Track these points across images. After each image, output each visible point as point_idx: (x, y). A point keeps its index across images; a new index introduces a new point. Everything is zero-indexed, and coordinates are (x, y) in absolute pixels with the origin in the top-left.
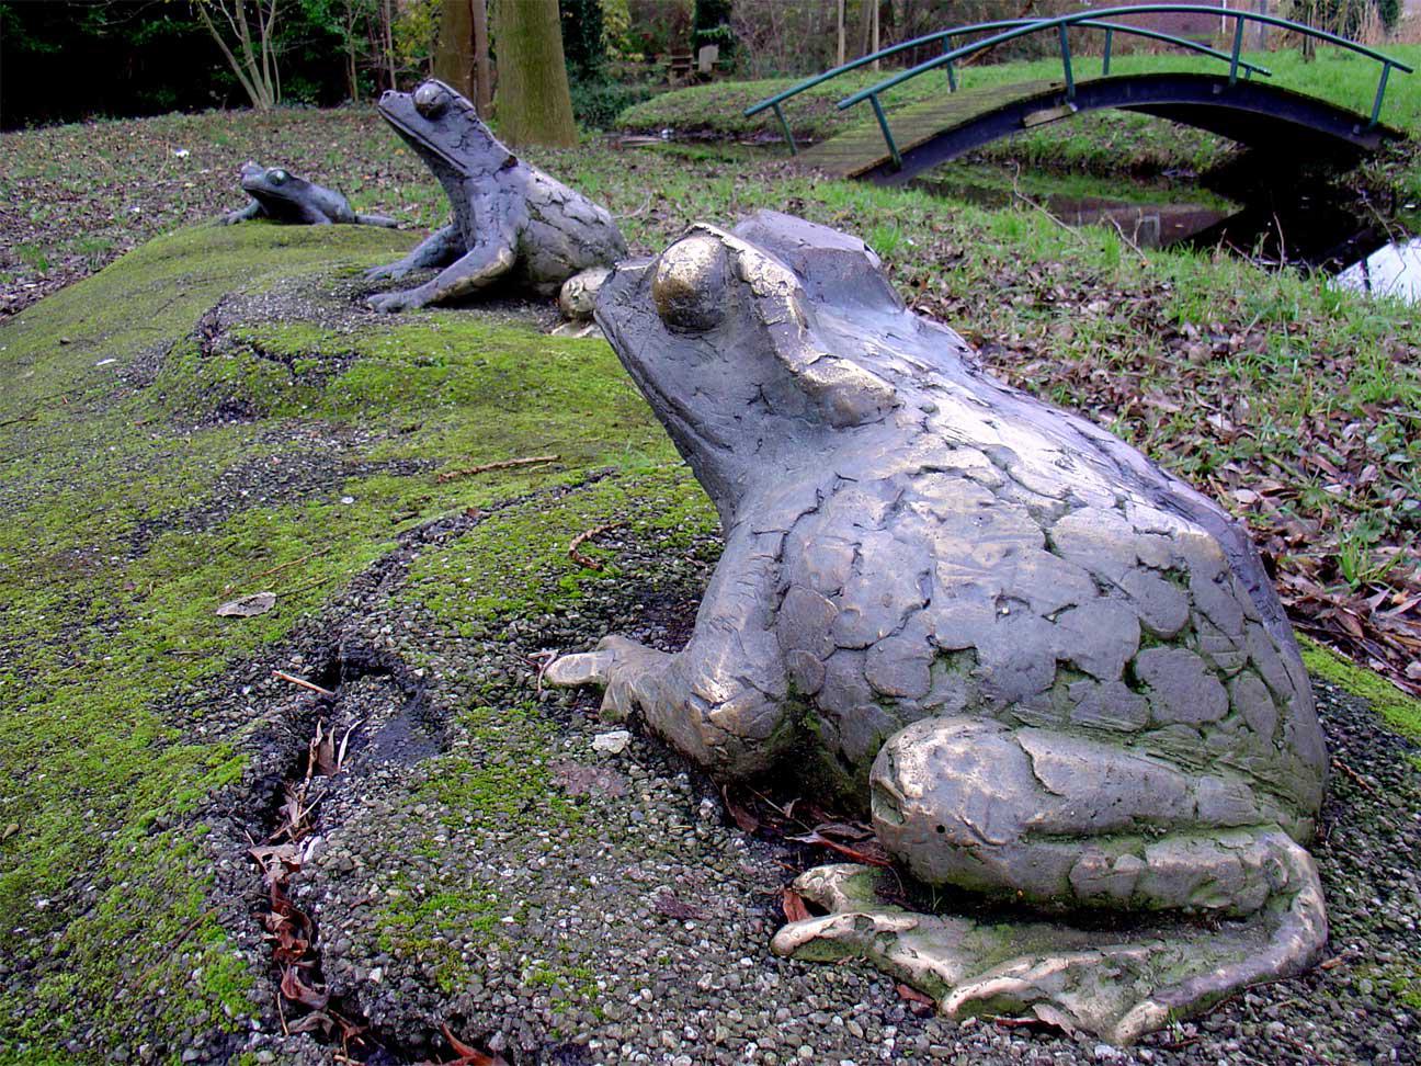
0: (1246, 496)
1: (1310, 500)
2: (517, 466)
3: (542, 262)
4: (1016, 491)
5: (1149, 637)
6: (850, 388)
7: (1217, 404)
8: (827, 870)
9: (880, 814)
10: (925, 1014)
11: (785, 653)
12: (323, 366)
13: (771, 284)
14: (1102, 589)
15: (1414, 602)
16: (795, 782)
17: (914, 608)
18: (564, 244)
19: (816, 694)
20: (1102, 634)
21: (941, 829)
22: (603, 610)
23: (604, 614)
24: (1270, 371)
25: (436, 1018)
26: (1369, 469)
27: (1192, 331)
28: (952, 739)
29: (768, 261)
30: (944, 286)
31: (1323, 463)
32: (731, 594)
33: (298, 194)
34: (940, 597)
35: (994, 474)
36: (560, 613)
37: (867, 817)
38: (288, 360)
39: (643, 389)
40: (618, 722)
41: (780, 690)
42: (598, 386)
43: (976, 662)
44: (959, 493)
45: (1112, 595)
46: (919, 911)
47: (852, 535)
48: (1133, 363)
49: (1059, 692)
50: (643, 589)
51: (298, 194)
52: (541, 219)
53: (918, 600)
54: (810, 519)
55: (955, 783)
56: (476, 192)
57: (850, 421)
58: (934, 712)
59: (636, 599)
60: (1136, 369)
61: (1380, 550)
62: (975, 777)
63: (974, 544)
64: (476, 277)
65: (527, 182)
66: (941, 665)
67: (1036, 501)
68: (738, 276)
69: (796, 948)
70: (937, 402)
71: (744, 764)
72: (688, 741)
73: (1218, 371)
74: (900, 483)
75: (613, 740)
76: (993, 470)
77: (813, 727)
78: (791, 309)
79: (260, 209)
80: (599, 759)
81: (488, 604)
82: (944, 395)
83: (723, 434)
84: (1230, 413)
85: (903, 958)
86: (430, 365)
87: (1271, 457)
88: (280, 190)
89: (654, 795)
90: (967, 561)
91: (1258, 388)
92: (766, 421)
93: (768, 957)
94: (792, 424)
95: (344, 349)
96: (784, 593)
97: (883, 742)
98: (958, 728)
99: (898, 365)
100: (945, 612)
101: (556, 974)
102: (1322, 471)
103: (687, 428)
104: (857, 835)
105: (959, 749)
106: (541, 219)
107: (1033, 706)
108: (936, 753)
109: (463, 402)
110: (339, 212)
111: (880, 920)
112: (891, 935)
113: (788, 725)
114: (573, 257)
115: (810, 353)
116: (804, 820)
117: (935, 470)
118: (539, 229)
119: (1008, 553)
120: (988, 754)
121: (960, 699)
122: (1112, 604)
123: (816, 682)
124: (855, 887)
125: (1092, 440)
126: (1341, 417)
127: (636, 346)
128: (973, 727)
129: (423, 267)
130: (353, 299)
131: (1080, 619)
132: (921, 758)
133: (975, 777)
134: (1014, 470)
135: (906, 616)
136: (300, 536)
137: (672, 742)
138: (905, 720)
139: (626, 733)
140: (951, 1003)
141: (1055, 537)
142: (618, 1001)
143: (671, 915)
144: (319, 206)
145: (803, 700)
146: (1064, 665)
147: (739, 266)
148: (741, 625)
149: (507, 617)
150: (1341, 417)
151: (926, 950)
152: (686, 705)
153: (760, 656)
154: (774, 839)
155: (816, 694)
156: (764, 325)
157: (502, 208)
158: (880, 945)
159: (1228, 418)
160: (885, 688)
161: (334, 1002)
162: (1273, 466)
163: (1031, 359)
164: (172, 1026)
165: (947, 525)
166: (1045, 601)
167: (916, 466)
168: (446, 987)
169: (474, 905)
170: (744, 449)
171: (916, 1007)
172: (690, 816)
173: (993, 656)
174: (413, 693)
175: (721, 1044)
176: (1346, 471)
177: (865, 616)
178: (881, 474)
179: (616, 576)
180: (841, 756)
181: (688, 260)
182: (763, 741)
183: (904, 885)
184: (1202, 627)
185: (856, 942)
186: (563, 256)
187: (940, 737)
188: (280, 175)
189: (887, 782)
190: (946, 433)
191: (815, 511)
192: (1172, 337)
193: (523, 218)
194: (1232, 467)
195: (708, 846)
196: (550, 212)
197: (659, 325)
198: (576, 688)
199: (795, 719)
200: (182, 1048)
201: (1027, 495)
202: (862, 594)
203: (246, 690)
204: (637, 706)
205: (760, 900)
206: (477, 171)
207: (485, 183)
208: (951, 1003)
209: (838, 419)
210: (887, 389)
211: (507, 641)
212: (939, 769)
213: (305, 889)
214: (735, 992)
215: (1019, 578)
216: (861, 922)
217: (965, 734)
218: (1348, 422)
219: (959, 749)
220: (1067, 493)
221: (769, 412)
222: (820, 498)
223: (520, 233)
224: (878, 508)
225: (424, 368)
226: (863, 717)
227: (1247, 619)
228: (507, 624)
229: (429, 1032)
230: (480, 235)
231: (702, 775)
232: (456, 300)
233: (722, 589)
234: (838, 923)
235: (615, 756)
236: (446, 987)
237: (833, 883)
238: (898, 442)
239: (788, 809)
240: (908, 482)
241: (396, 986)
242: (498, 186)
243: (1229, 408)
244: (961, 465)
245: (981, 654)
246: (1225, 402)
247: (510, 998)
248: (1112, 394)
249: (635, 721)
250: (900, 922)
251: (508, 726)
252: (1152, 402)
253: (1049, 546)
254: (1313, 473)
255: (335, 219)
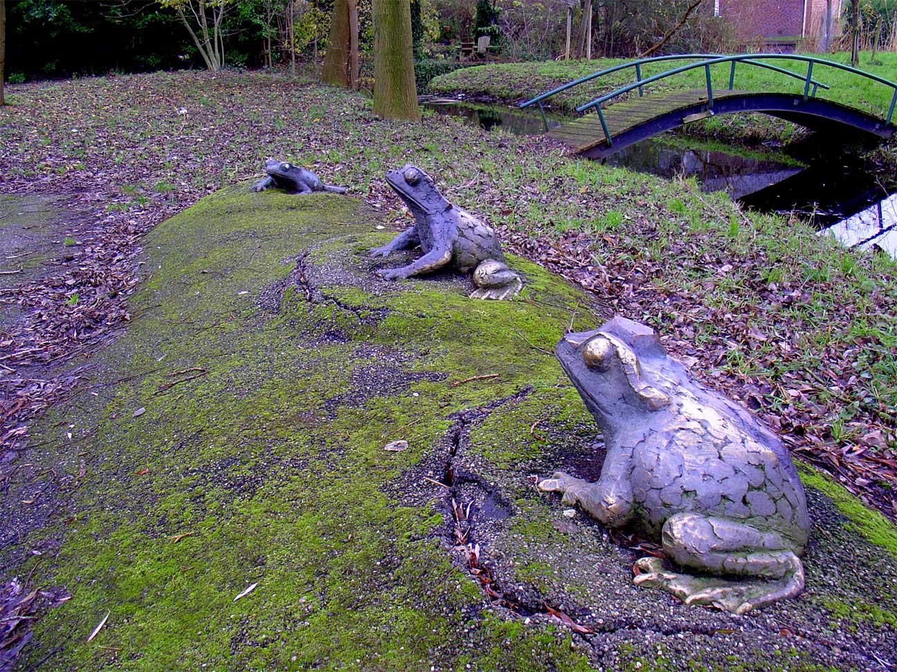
0: (794, 393)
1: (823, 396)
2: (481, 379)
3: (463, 257)
4: (709, 437)
5: (751, 488)
6: (655, 399)
7: (784, 335)
8: (647, 559)
9: (665, 542)
10: (680, 604)
11: (633, 488)
12: (374, 315)
13: (629, 360)
14: (736, 472)
15: (862, 450)
16: (637, 530)
17: (677, 477)
18: (475, 249)
19: (643, 502)
20: (736, 487)
21: (685, 548)
22: (549, 459)
23: (550, 460)
24: (811, 315)
25: (541, 601)
26: (853, 378)
27: (774, 287)
28: (689, 520)
29: (627, 350)
30: (648, 254)
31: (831, 373)
32: (614, 466)
33: (295, 175)
34: (685, 474)
35: (702, 431)
36: (534, 460)
37: (660, 542)
38: (354, 309)
39: (577, 388)
40: (571, 506)
41: (631, 500)
42: (503, 331)
43: (696, 495)
44: (691, 438)
45: (740, 474)
46: (677, 572)
47: (656, 451)
48: (744, 309)
49: (722, 506)
50: (562, 451)
51: (295, 175)
52: (464, 236)
53: (678, 475)
54: (642, 444)
55: (690, 534)
56: (433, 222)
57: (654, 409)
58: (682, 511)
59: (561, 455)
60: (745, 312)
61: (851, 424)
62: (696, 533)
63: (696, 457)
64: (433, 265)
65: (457, 218)
66: (685, 496)
67: (716, 441)
68: (617, 354)
69: (640, 583)
70: (683, 402)
71: (618, 523)
72: (599, 516)
73: (786, 314)
74: (672, 434)
75: (569, 513)
76: (702, 429)
77: (641, 512)
78: (635, 369)
79: (272, 181)
80: (566, 519)
81: (508, 455)
82: (683, 397)
83: (609, 409)
84: (790, 341)
85: (673, 587)
86: (423, 317)
87: (807, 369)
88: (286, 174)
89: (588, 532)
90: (694, 462)
91: (805, 326)
92: (624, 406)
93: (633, 585)
94: (634, 408)
95: (381, 306)
96: (633, 468)
97: (665, 520)
98: (690, 517)
99: (668, 385)
100: (687, 479)
101: (575, 588)
102: (831, 378)
103: (595, 405)
104: (654, 548)
105: (691, 524)
106: (464, 236)
107: (714, 510)
108: (684, 525)
109: (444, 338)
110: (315, 185)
111: (666, 575)
112: (669, 580)
113: (632, 511)
114: (478, 255)
115: (643, 386)
116: (635, 543)
117: (683, 429)
118: (463, 241)
119: (707, 460)
120: (700, 526)
121: (691, 507)
122: (739, 478)
123: (644, 499)
124: (656, 565)
125: (733, 410)
126: (843, 346)
127: (576, 372)
128: (695, 517)
129: (398, 250)
130: (370, 270)
131: (729, 482)
132: (680, 526)
133: (696, 533)
134: (709, 429)
135: (674, 480)
136: (404, 413)
137: (592, 514)
138: (673, 513)
139: (574, 511)
140: (688, 601)
141: (722, 454)
142: (595, 597)
143: (603, 572)
144: (305, 182)
145: (638, 504)
146: (724, 497)
147: (617, 352)
148: (619, 478)
149: (516, 461)
150: (843, 346)
151: (679, 584)
152: (600, 504)
153: (625, 489)
154: (626, 548)
155: (643, 502)
156: (626, 374)
157: (446, 230)
158: (665, 583)
159: (789, 344)
160: (666, 502)
161: (505, 596)
162: (808, 374)
163: (694, 304)
164: (454, 603)
165: (688, 449)
166: (718, 477)
167: (677, 428)
168: (543, 592)
169: (544, 567)
170: (616, 415)
171: (677, 601)
172: (600, 540)
173: (701, 493)
174: (492, 492)
175: (626, 609)
176: (842, 378)
177: (660, 477)
178: (665, 430)
179: (551, 444)
180: (650, 522)
181: (599, 347)
182: (624, 516)
183: (671, 563)
184: (768, 484)
185: (658, 581)
186: (474, 254)
187: (686, 520)
188: (287, 166)
189: (669, 533)
190: (685, 414)
191: (643, 441)
192: (764, 293)
193: (455, 236)
194: (789, 375)
195: (607, 551)
196: (468, 233)
197: (584, 367)
198: (551, 492)
199: (635, 510)
200: (460, 609)
201: (713, 439)
202: (659, 473)
203: (415, 485)
204: (578, 501)
205: (626, 568)
206: (434, 211)
207: (438, 218)
208: (688, 601)
209: (650, 409)
210: (663, 396)
211: (519, 471)
212: (685, 530)
213: (487, 562)
214: (626, 595)
215: (711, 468)
216: (660, 576)
217: (693, 519)
218: (846, 349)
219: (691, 524)
220: (726, 438)
221: (626, 403)
222: (645, 437)
223: (454, 243)
224: (665, 442)
225: (422, 319)
226: (659, 511)
227: (784, 480)
228: (517, 464)
229: (538, 605)
230: (436, 244)
231: (602, 526)
232: (424, 276)
233: (612, 465)
234: (652, 576)
235: (571, 518)
236: (543, 592)
237: (648, 563)
238: (670, 418)
239: (630, 538)
240: (674, 434)
241: (528, 591)
242: (443, 219)
243: (789, 338)
244: (692, 428)
245: (698, 493)
246: (788, 335)
247: (563, 595)
248: (734, 329)
249: (577, 505)
250: (671, 576)
251: (532, 506)
252: (753, 335)
253: (720, 458)
254: (826, 379)
255: (314, 189)
